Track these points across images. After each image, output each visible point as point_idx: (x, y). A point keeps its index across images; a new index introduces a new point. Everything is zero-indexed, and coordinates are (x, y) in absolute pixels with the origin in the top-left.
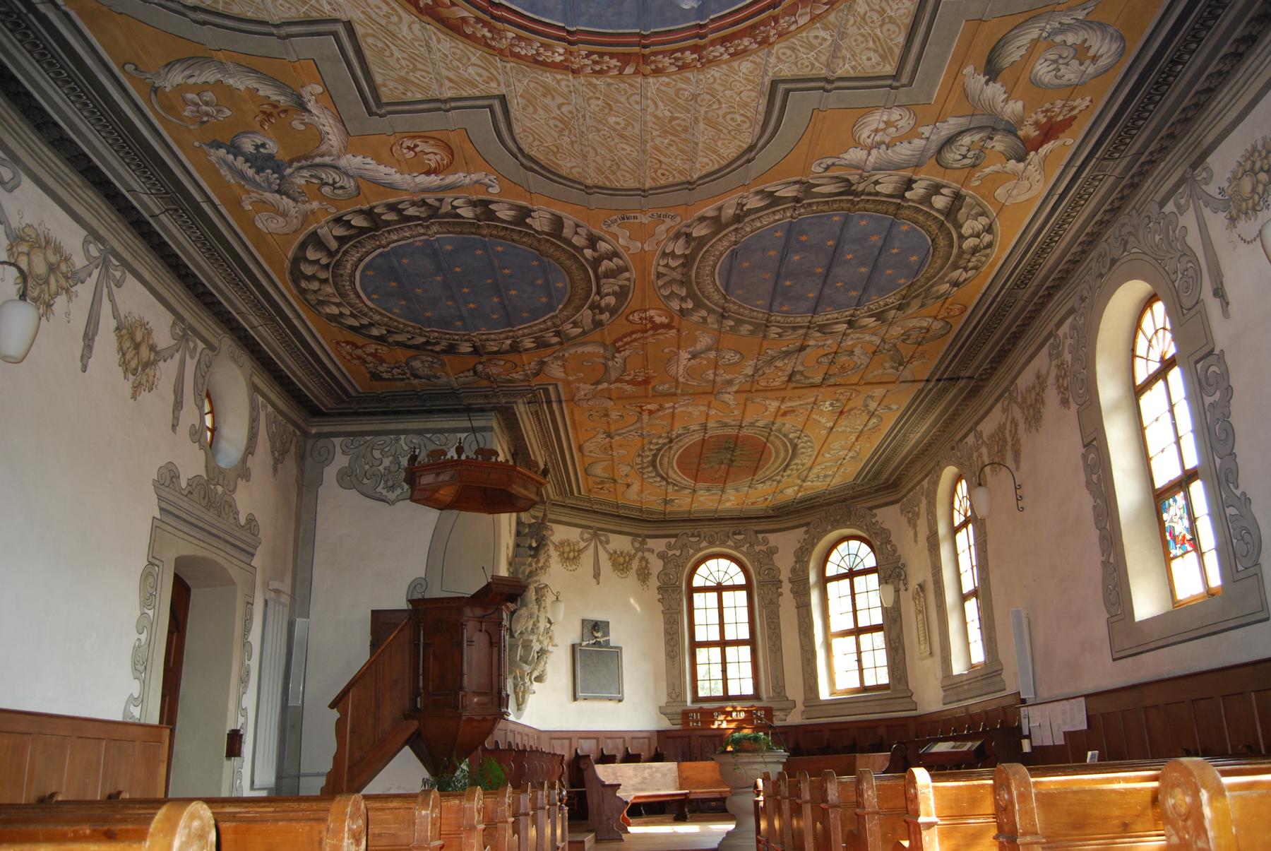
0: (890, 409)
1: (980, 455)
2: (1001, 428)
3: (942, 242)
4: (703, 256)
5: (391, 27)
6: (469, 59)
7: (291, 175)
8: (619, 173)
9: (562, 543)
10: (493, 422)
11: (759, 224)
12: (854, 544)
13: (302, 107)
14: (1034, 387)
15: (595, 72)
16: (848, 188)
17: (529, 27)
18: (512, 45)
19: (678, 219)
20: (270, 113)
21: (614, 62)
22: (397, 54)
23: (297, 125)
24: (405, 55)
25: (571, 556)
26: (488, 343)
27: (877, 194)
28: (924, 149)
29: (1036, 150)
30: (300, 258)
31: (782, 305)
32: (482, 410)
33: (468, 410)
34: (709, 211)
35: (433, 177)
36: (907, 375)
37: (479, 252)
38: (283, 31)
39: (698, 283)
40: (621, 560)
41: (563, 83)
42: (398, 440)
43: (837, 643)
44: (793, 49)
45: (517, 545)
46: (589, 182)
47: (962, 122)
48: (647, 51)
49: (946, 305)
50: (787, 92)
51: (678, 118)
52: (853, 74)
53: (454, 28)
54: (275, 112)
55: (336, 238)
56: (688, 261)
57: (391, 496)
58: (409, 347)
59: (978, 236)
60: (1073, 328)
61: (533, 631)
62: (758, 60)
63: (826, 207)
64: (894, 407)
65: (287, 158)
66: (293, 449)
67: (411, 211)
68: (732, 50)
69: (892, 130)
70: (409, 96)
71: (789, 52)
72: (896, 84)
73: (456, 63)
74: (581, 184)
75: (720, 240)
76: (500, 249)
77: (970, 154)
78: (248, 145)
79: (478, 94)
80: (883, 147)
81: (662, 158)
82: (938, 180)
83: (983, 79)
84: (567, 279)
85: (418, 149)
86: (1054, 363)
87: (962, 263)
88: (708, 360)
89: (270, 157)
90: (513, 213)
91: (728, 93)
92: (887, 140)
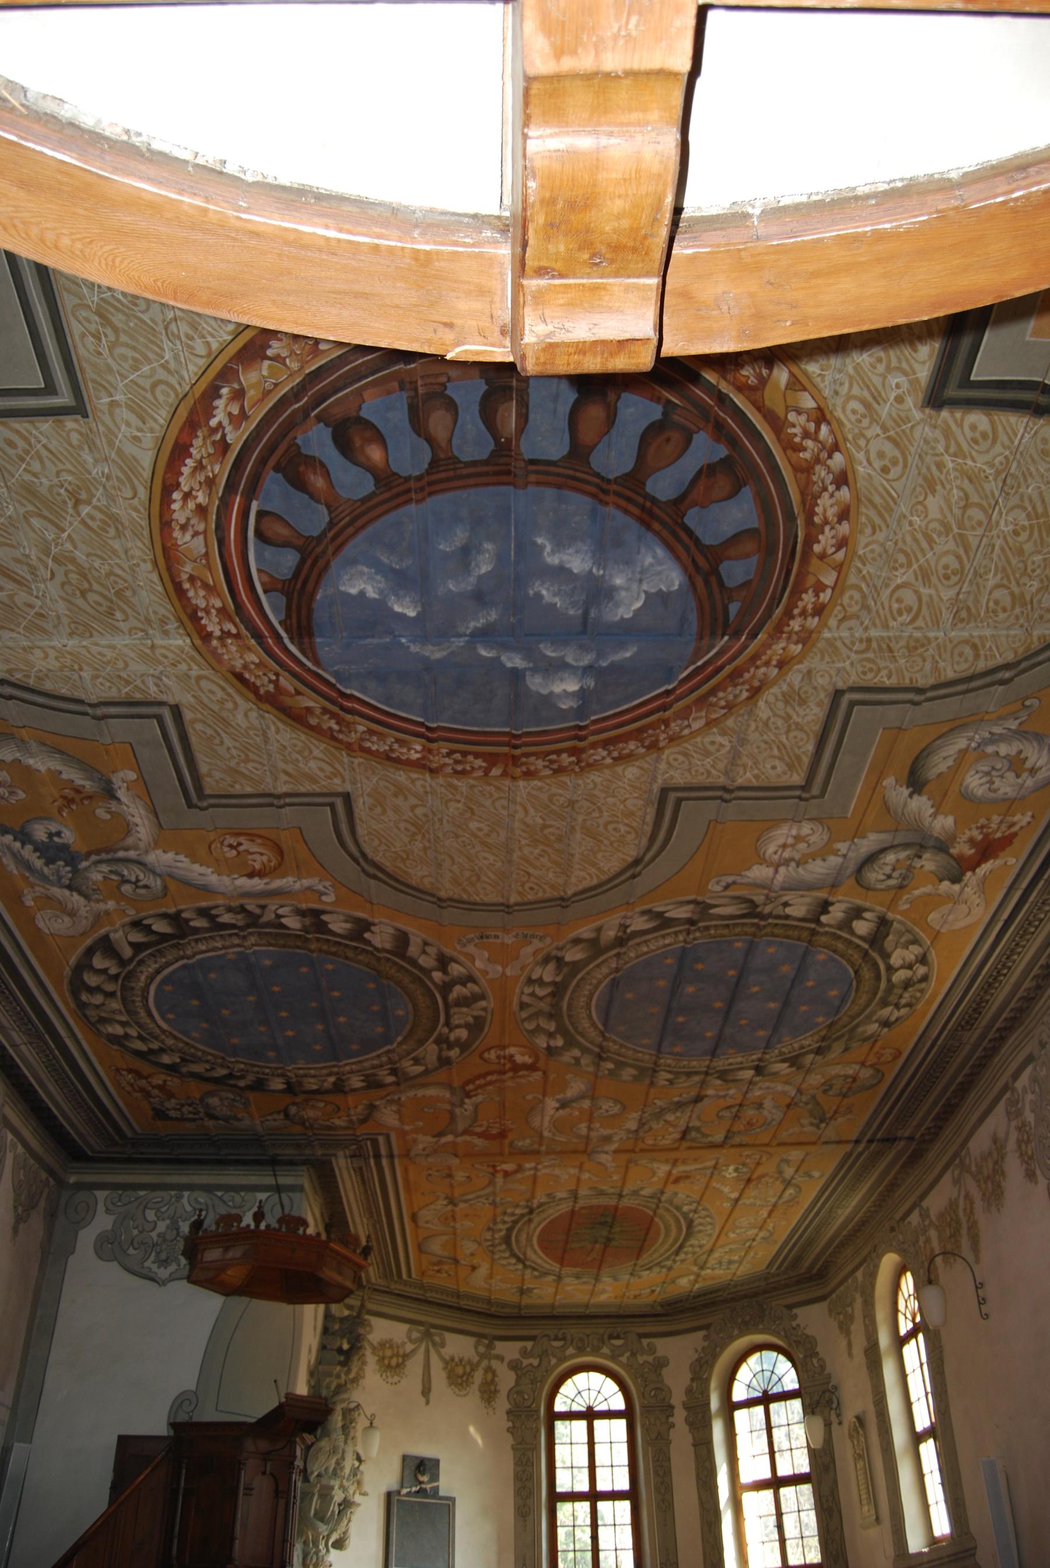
0: (811, 1177)
1: (928, 1241)
2: (953, 1205)
3: (867, 974)
4: (578, 985)
5: (224, 714)
6: (311, 752)
7: (86, 869)
9: (382, 1345)
10: (304, 1179)
11: (645, 949)
12: (770, 1355)
13: (110, 793)
14: (990, 1154)
15: (456, 772)
16: (752, 910)
17: (382, 721)
18: (362, 739)
19: (548, 940)
20: (73, 799)
21: (479, 762)
22: (228, 742)
23: (102, 813)
24: (237, 745)
25: (393, 1363)
26: (306, 1080)
27: (787, 917)
28: (841, 868)
29: (973, 870)
30: (84, 965)
32: (291, 1163)
33: (274, 1163)
34: (585, 932)
35: (256, 881)
36: (830, 1133)
37: (304, 970)
38: (100, 711)
39: (570, 1016)
40: (460, 1370)
41: (419, 783)
42: (179, 1198)
43: (749, 1499)
44: (686, 755)
45: (323, 1347)
46: (442, 894)
47: (885, 838)
48: (517, 752)
49: (875, 1049)
50: (679, 802)
51: (550, 826)
52: (755, 783)
53: (297, 718)
54: (77, 798)
55: (131, 944)
56: (558, 990)
57: (163, 1273)
58: (207, 1080)
59: (910, 967)
60: (1034, 1080)
61: (335, 1473)
62: (646, 766)
63: (726, 931)
64: (816, 1174)
65: (84, 850)
66: (42, 1204)
67: (226, 918)
68: (615, 754)
69: (802, 846)
70: (238, 789)
71: (681, 758)
72: (805, 795)
73: (295, 756)
74: (433, 895)
75: (598, 966)
76: (329, 967)
77: (896, 874)
78: (40, 832)
79: (318, 790)
80: (793, 864)
81: (531, 870)
82: (859, 902)
83: (906, 792)
84: (410, 1007)
85: (241, 848)
86: (1014, 1124)
87: (893, 998)
89: (65, 847)
90: (348, 926)
91: (610, 800)
92: (797, 856)
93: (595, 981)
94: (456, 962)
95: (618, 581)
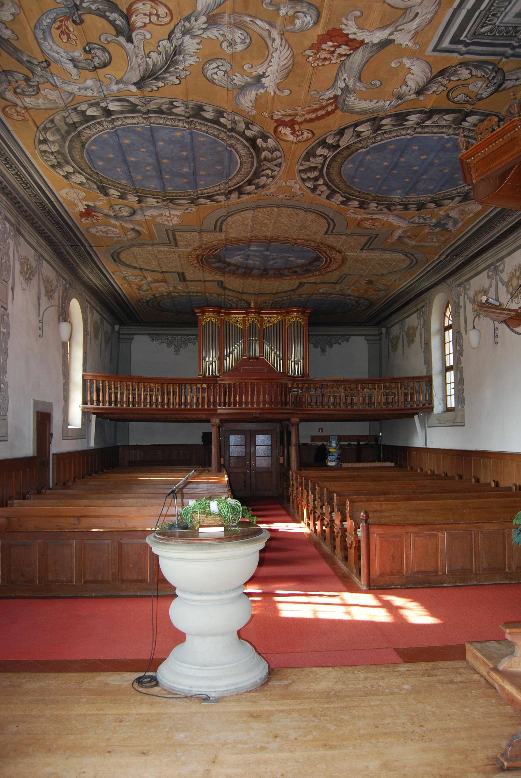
4: (248, 174)
8: (289, 213)
11: (215, 188)
19: (263, 194)
31: (183, 137)
34: (245, 197)
39: (252, 158)
56: (257, 174)
63: (180, 194)
75: (238, 183)
84: (343, 168)
88: (243, 72)
90: (350, 203)
93: (239, 176)
94: (309, 188)
95: (241, 260)
